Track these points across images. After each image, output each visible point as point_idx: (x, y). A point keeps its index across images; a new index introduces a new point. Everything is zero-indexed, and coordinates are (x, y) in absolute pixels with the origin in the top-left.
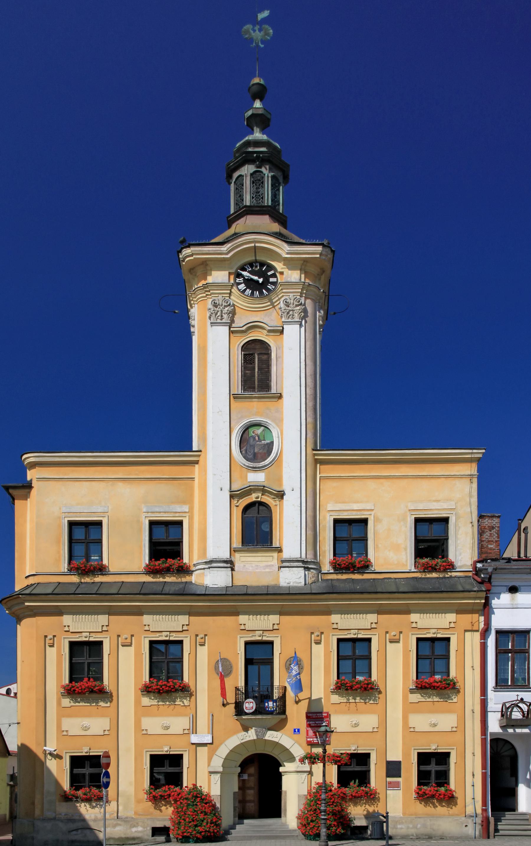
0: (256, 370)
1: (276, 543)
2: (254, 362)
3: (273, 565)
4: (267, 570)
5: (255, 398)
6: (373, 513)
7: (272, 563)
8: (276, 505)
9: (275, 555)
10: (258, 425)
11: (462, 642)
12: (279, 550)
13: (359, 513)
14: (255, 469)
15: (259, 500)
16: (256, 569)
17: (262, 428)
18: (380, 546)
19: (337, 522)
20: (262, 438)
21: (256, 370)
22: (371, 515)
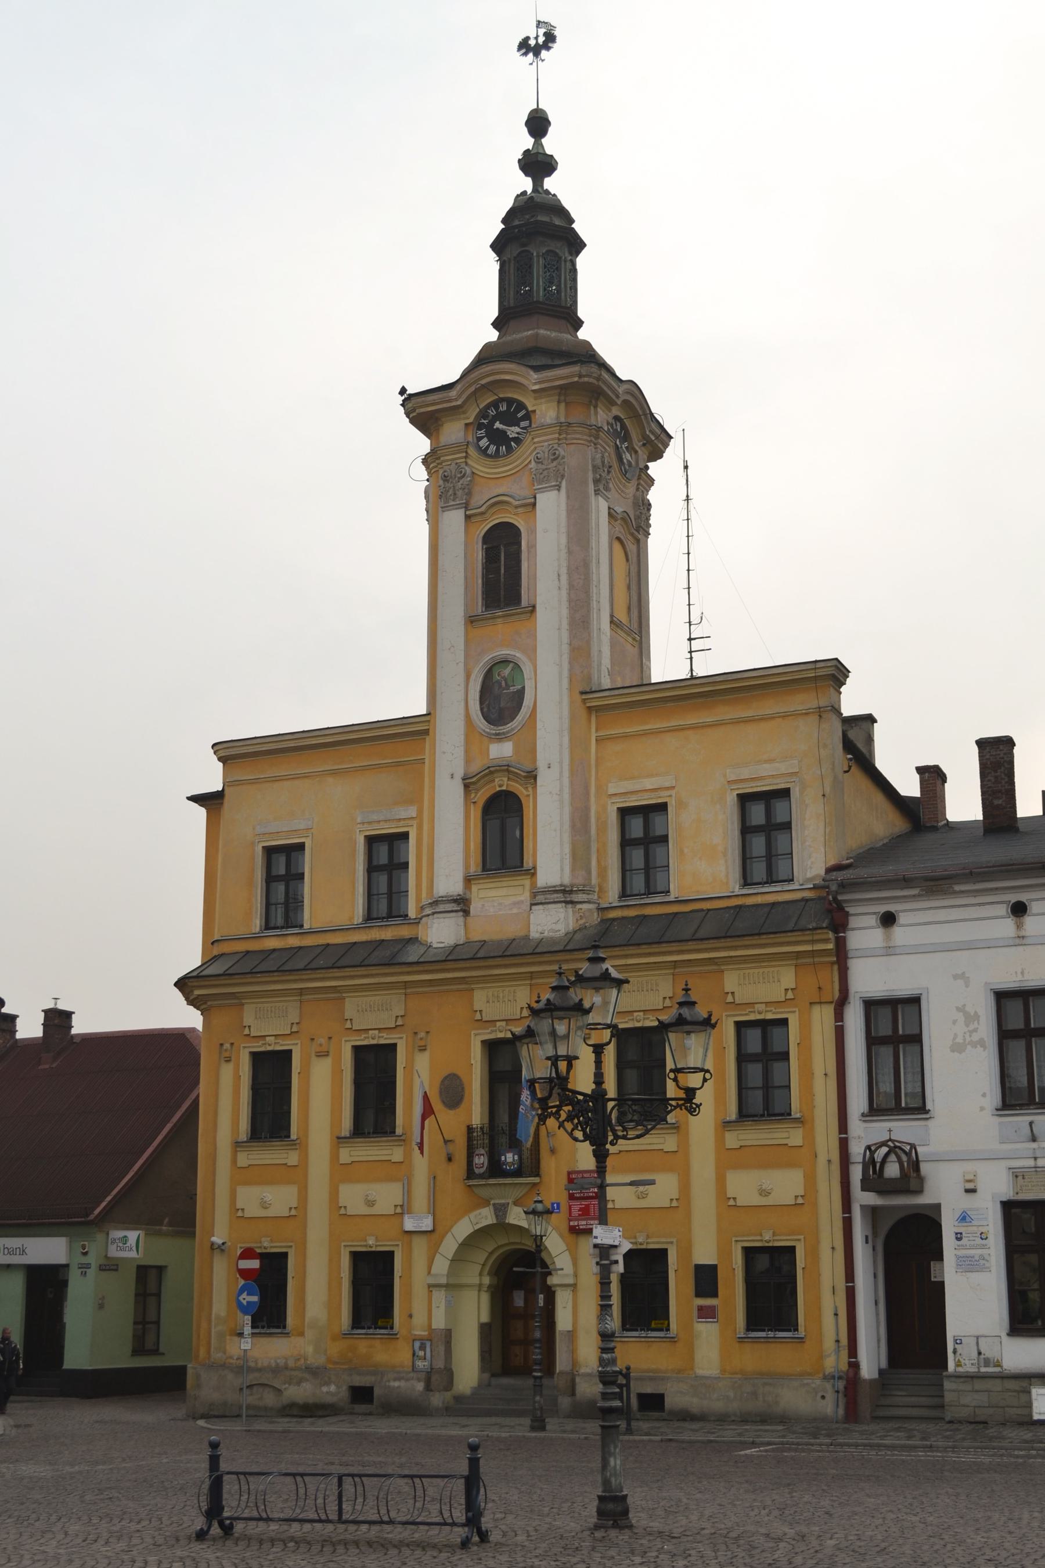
0: (503, 571)
1: (528, 863)
2: (499, 560)
3: (522, 902)
4: (515, 911)
5: (499, 617)
6: (673, 792)
7: (522, 898)
8: (528, 796)
9: (527, 882)
10: (505, 662)
11: (806, 1027)
12: (532, 873)
13: (653, 795)
14: (500, 740)
15: (504, 788)
16: (503, 910)
17: (511, 665)
18: (686, 850)
19: (625, 813)
20: (510, 683)
21: (503, 571)
22: (670, 796)
